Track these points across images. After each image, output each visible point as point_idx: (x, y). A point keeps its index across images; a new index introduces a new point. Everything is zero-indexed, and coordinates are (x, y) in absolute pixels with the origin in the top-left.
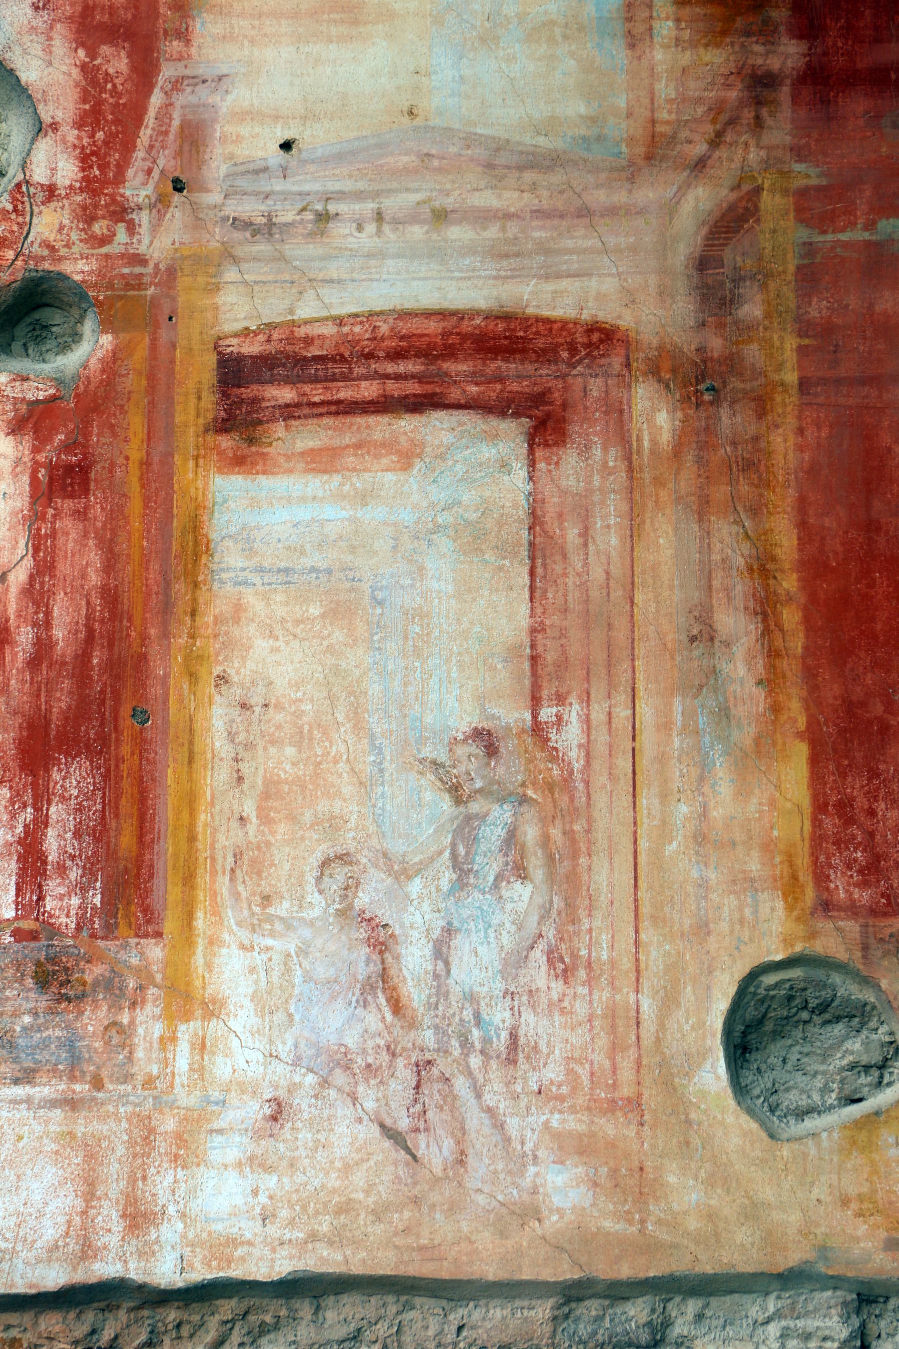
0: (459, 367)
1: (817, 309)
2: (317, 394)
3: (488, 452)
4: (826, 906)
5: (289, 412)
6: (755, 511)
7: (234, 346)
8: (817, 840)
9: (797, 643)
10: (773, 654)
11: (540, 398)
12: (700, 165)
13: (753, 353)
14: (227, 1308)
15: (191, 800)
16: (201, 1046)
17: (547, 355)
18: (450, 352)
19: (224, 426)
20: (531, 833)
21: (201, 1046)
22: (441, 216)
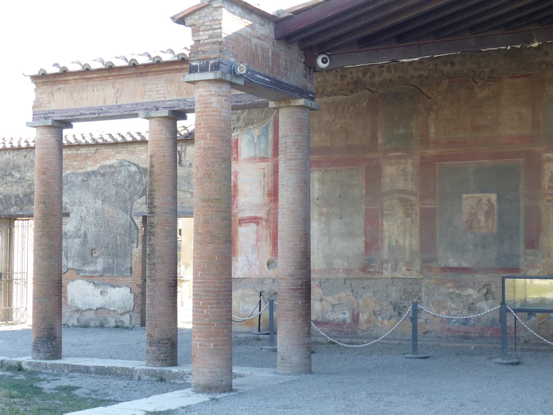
0: (252, 220)
1: (274, 216)
2: (245, 222)
3: (254, 226)
4: (273, 256)
5: (243, 223)
6: (270, 230)
7: (240, 218)
8: (272, 252)
9: (272, 239)
10: (270, 239)
11: (257, 222)
12: (267, 206)
13: (270, 219)
14: (240, 279)
15: (237, 248)
16: (238, 264)
17: (258, 219)
18: (252, 219)
19: (239, 224)
20: (256, 251)
21: (238, 264)
22: (252, 210)
